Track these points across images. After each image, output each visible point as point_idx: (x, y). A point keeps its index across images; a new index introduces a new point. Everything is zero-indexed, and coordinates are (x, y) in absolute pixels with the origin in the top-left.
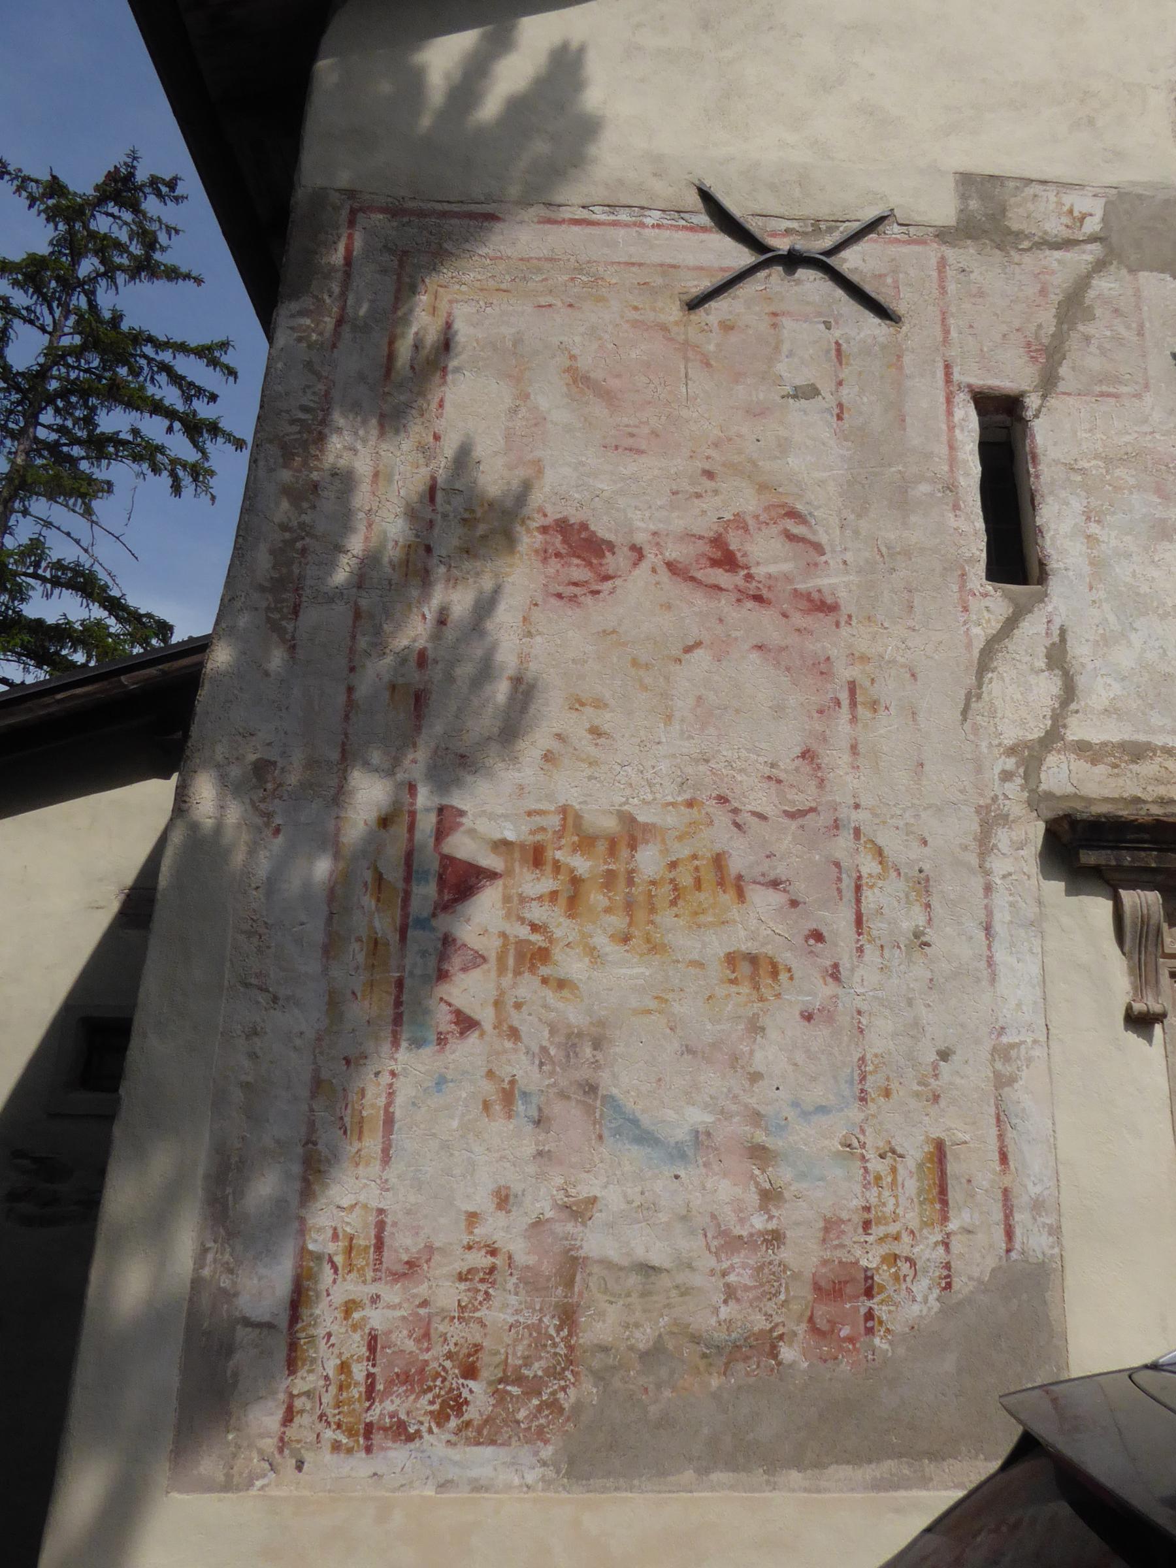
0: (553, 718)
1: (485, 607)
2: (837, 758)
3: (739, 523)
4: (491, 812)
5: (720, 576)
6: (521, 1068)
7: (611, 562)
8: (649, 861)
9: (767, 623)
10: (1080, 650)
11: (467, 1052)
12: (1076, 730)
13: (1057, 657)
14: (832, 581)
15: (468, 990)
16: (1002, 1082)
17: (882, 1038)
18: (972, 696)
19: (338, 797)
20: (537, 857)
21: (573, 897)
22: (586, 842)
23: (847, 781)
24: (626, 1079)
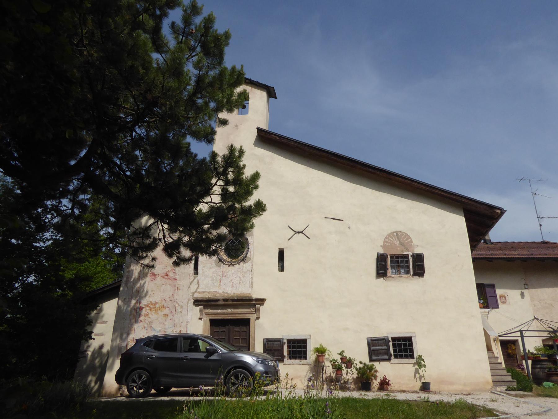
0: (150, 292)
1: (144, 283)
2: (175, 295)
3: (169, 271)
4: (144, 302)
5: (166, 277)
6: (146, 325)
7: (156, 276)
8: (157, 306)
9: (170, 282)
10: (200, 282)
11: (141, 324)
12: (199, 290)
13: (198, 283)
14: (177, 277)
15: (142, 318)
16: (187, 325)
17: (177, 321)
18: (189, 287)
19: (130, 301)
20: (148, 306)
21: (151, 309)
22: (152, 304)
23: (176, 297)
24: (154, 326)
